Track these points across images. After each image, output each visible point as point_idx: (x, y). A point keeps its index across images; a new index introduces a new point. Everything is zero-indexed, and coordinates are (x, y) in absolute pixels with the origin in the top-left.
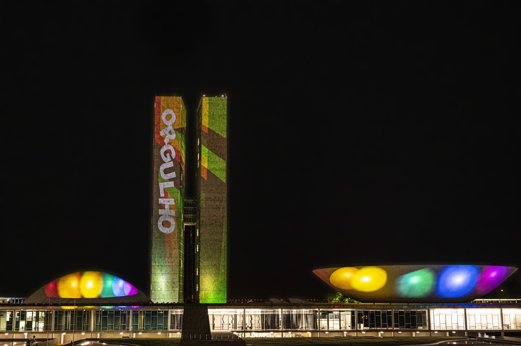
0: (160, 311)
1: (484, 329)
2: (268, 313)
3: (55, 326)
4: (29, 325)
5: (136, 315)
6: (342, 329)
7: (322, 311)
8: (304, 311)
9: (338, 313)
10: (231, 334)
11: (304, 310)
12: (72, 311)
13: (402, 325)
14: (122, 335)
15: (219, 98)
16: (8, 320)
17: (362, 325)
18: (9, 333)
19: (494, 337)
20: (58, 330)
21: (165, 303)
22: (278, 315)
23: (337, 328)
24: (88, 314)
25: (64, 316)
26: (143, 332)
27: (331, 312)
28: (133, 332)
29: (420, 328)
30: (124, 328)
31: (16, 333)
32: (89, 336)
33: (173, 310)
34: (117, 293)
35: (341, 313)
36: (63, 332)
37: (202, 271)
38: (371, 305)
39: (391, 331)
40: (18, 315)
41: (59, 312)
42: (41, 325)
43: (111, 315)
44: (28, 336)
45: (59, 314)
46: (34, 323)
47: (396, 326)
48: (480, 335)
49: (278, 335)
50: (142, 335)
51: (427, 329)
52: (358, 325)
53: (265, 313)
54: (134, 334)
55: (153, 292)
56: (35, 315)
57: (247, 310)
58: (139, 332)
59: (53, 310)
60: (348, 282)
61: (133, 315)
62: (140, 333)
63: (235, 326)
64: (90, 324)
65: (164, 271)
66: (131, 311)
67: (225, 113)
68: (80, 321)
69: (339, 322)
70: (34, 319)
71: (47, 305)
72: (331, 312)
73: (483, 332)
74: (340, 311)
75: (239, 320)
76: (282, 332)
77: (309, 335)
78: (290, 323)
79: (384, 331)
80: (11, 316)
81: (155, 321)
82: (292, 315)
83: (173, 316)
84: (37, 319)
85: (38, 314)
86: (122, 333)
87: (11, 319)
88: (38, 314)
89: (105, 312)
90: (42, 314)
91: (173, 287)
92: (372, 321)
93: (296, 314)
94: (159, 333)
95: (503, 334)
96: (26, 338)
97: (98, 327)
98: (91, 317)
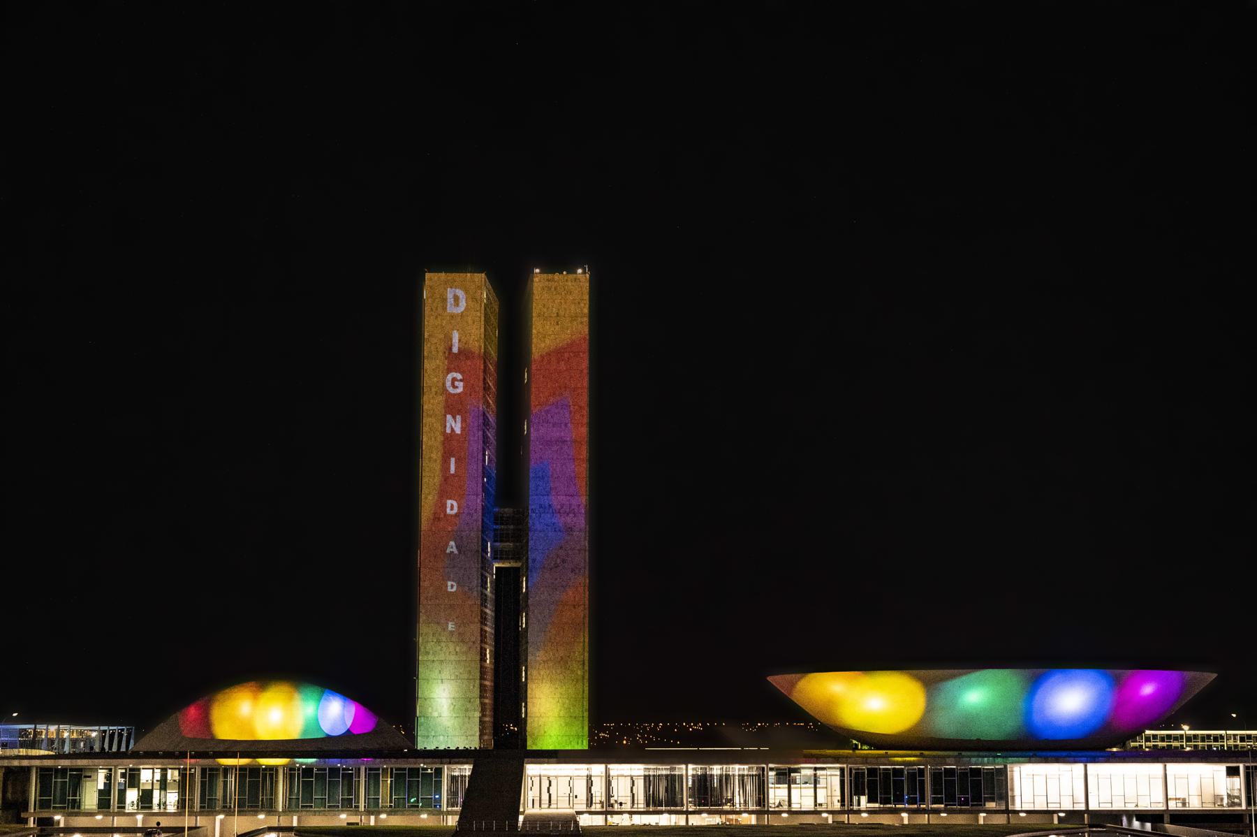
0: (424, 769)
1: (1131, 807)
2: (659, 773)
3: (203, 801)
4: (146, 798)
5: (373, 776)
6: (819, 809)
7: (777, 769)
8: (736, 769)
9: (811, 772)
10: (571, 820)
11: (737, 766)
12: (242, 768)
13: (950, 799)
14: (343, 819)
15: (571, 276)
16: (101, 786)
17: (864, 799)
18: (106, 815)
19: (1148, 826)
20: (208, 807)
21: (442, 748)
23: (808, 805)
24: (271, 775)
26: (389, 814)
28: (369, 813)
29: (991, 805)
30: (349, 805)
31: (119, 814)
32: (274, 821)
33: (454, 766)
35: (819, 772)
36: (219, 813)
37: (533, 673)
38: (879, 757)
39: (924, 811)
40: (123, 775)
41: (211, 769)
42: (172, 797)
43: (321, 777)
44: (144, 821)
45: (210, 775)
46: (156, 794)
47: (935, 801)
49: (680, 820)
50: (386, 820)
51: (1003, 808)
52: (855, 798)
54: (372, 818)
55: (421, 720)
56: (158, 776)
57: (610, 766)
58: (379, 813)
59: (195, 766)
60: (831, 703)
61: (368, 776)
62: (383, 816)
63: (590, 801)
64: (276, 794)
65: (446, 674)
66: (363, 769)
67: (586, 311)
68: (254, 793)
69: (816, 790)
70: (157, 786)
71: (183, 755)
72: (796, 771)
74: (816, 769)
75: (598, 790)
76: (687, 813)
77: (753, 820)
78: (706, 794)
79: (910, 812)
80: (108, 778)
81: (415, 788)
82: (712, 776)
83: (454, 779)
84: (164, 785)
85: (164, 776)
86: (343, 816)
87: (108, 786)
88: (164, 776)
89: (308, 771)
90: (173, 775)
91: (467, 710)
92: (886, 791)
93: (721, 776)
94: (424, 816)
96: (140, 825)
97: (294, 802)
98: (277, 782)
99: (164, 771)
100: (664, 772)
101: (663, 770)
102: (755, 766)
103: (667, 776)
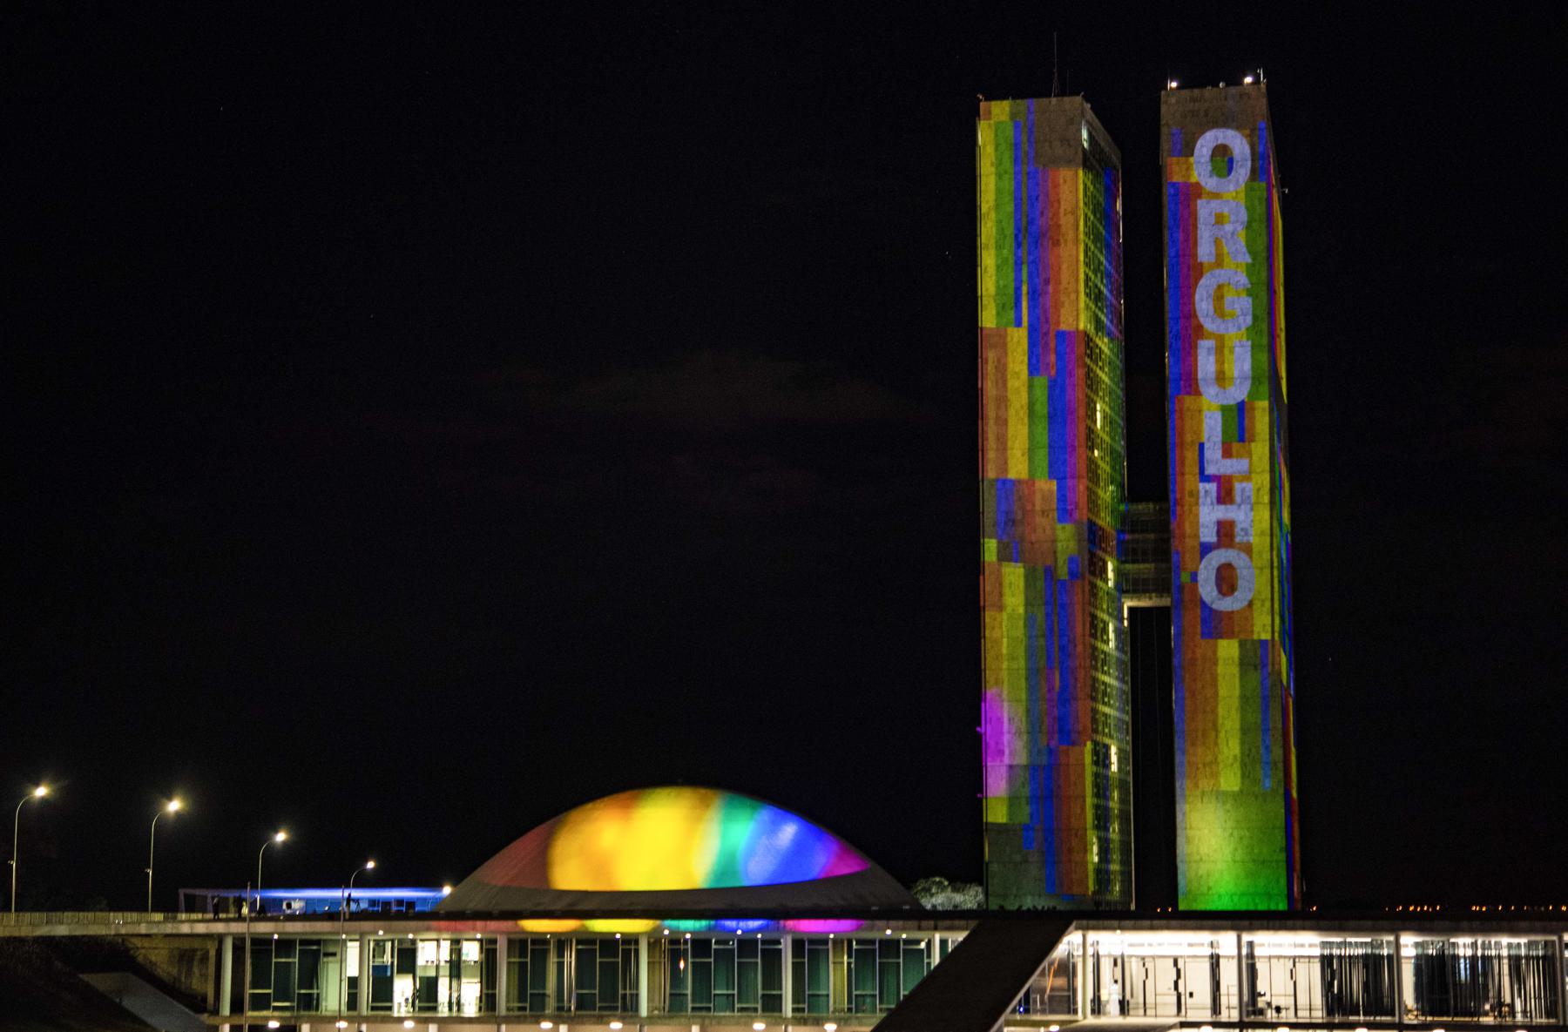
4: (427, 993)
8: (1504, 944)
11: (1505, 940)
22: (1394, 960)
25: (552, 959)
34: (757, 872)
42: (471, 991)
53: (1336, 952)
70: (445, 971)
82: (1456, 958)
84: (456, 968)
89: (700, 945)
90: (471, 952)
93: (1474, 958)
99: (456, 943)
100: (1360, 951)
101: (1356, 944)
102: (1539, 938)
103: (1365, 957)
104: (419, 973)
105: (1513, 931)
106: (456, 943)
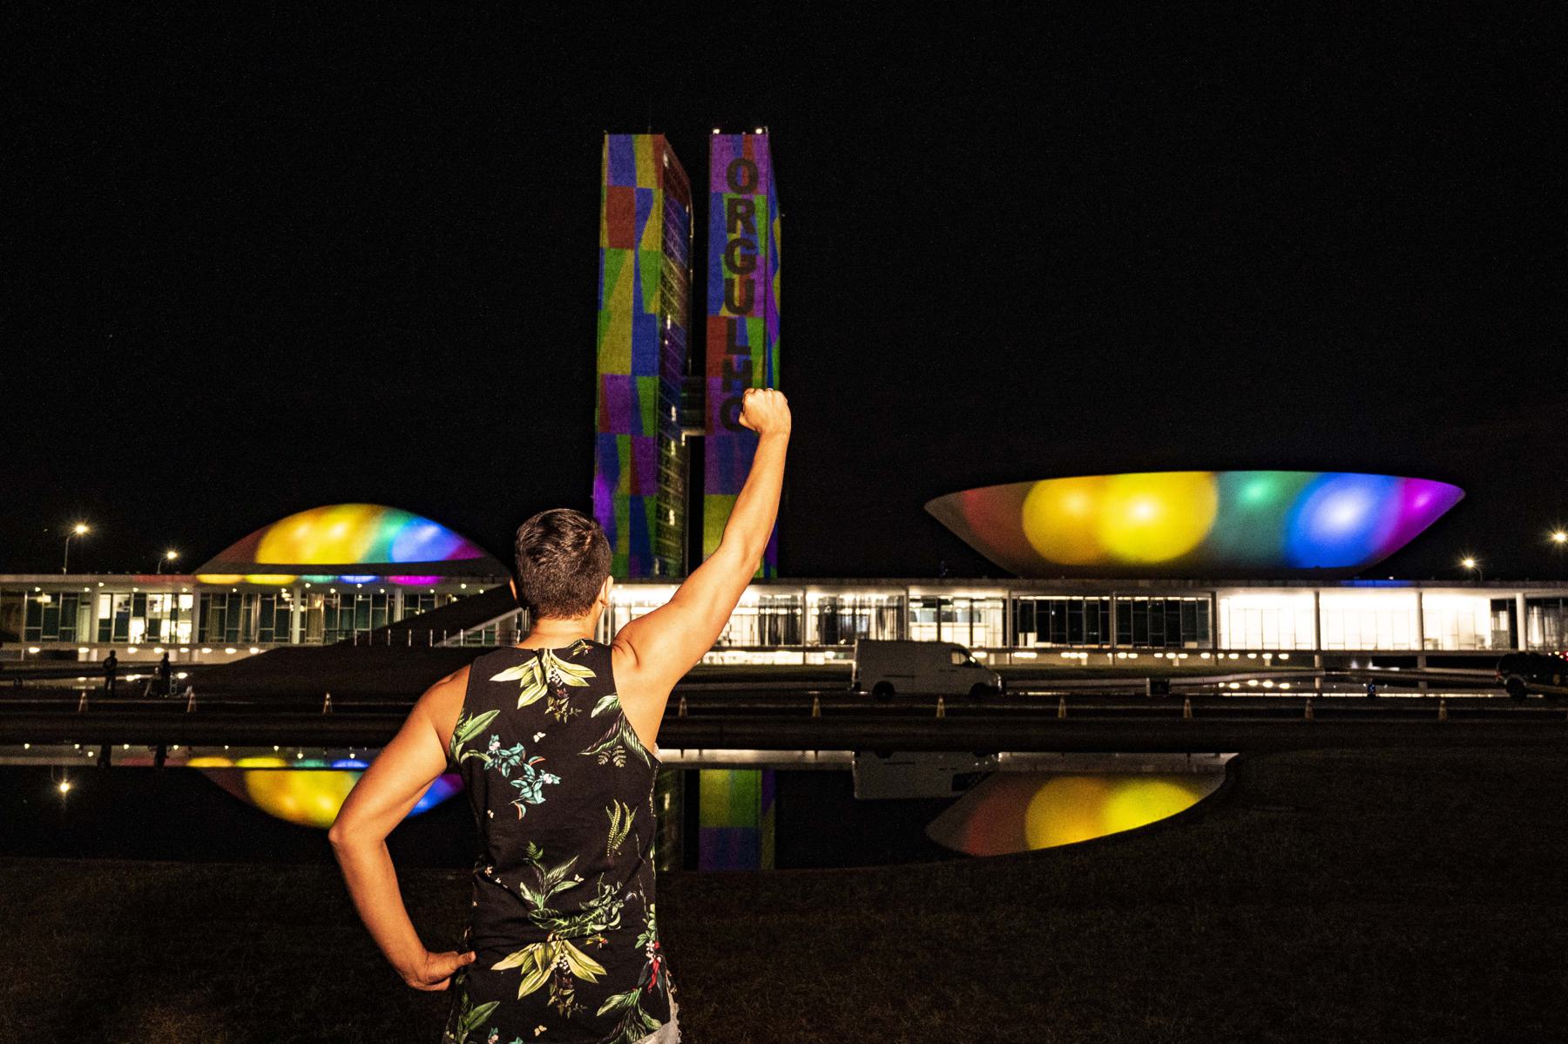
1: (1369, 647)
4: (154, 627)
9: (967, 604)
17: (1032, 637)
25: (243, 607)
27: (946, 602)
35: (976, 605)
42: (185, 631)
48: (1354, 666)
73: (1362, 656)
74: (972, 600)
84: (175, 615)
90: (186, 602)
92: (1061, 628)
95: (1421, 662)
99: (176, 596)
101: (782, 596)
104: (149, 616)
105: (879, 587)
106: (176, 596)
